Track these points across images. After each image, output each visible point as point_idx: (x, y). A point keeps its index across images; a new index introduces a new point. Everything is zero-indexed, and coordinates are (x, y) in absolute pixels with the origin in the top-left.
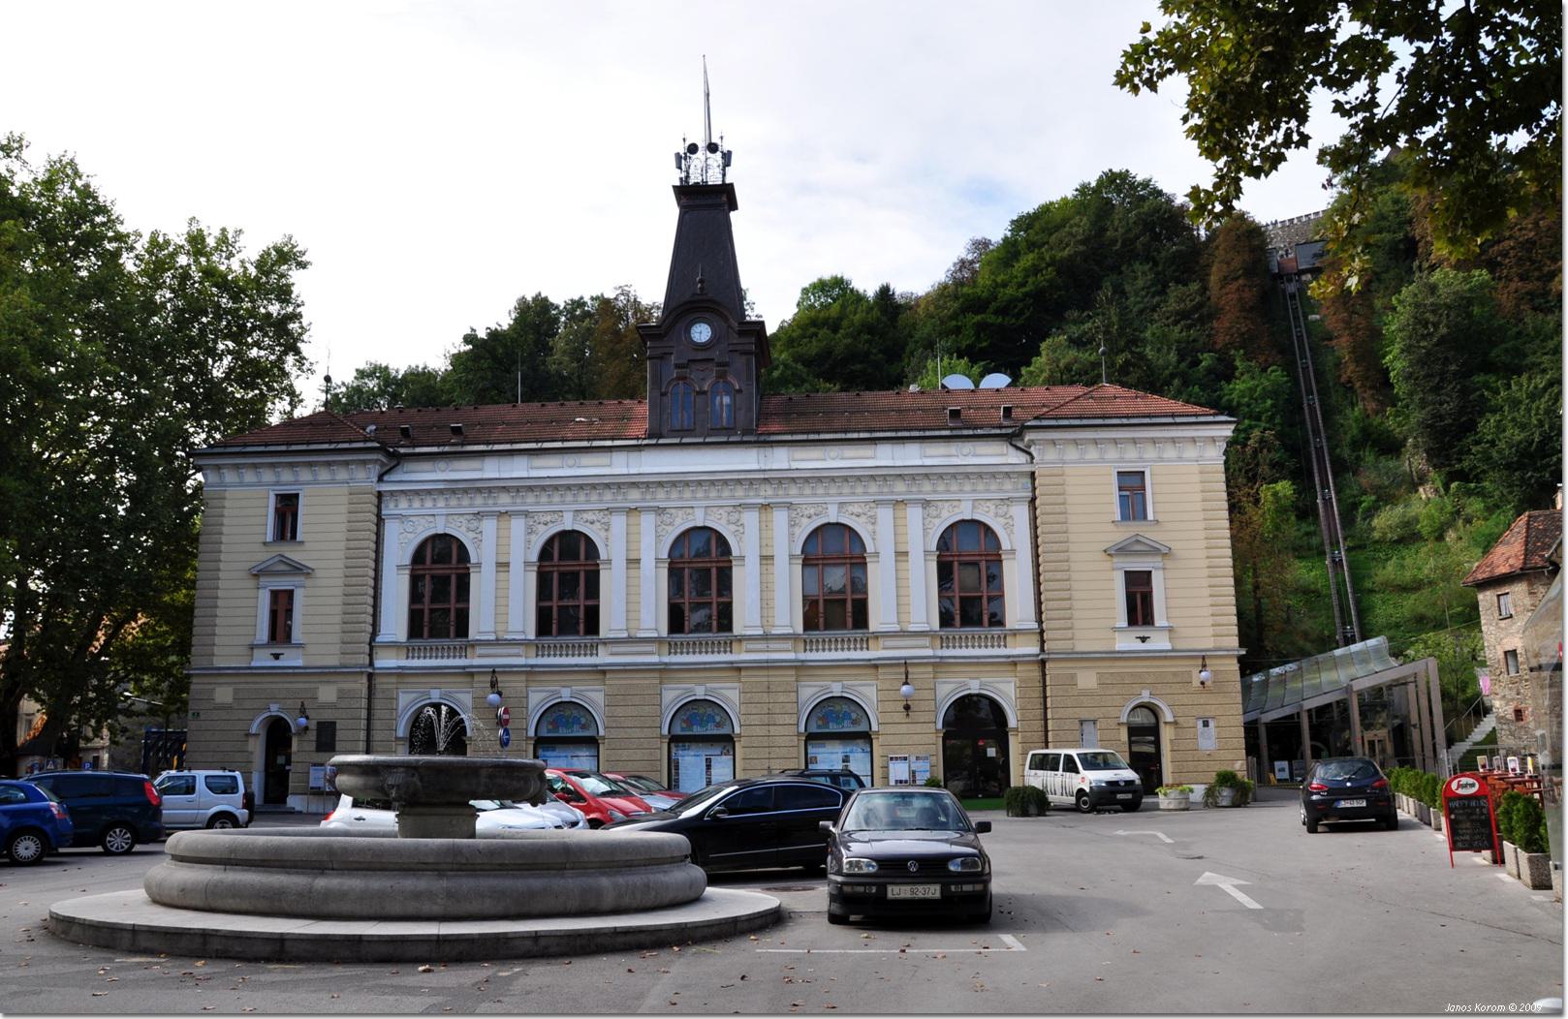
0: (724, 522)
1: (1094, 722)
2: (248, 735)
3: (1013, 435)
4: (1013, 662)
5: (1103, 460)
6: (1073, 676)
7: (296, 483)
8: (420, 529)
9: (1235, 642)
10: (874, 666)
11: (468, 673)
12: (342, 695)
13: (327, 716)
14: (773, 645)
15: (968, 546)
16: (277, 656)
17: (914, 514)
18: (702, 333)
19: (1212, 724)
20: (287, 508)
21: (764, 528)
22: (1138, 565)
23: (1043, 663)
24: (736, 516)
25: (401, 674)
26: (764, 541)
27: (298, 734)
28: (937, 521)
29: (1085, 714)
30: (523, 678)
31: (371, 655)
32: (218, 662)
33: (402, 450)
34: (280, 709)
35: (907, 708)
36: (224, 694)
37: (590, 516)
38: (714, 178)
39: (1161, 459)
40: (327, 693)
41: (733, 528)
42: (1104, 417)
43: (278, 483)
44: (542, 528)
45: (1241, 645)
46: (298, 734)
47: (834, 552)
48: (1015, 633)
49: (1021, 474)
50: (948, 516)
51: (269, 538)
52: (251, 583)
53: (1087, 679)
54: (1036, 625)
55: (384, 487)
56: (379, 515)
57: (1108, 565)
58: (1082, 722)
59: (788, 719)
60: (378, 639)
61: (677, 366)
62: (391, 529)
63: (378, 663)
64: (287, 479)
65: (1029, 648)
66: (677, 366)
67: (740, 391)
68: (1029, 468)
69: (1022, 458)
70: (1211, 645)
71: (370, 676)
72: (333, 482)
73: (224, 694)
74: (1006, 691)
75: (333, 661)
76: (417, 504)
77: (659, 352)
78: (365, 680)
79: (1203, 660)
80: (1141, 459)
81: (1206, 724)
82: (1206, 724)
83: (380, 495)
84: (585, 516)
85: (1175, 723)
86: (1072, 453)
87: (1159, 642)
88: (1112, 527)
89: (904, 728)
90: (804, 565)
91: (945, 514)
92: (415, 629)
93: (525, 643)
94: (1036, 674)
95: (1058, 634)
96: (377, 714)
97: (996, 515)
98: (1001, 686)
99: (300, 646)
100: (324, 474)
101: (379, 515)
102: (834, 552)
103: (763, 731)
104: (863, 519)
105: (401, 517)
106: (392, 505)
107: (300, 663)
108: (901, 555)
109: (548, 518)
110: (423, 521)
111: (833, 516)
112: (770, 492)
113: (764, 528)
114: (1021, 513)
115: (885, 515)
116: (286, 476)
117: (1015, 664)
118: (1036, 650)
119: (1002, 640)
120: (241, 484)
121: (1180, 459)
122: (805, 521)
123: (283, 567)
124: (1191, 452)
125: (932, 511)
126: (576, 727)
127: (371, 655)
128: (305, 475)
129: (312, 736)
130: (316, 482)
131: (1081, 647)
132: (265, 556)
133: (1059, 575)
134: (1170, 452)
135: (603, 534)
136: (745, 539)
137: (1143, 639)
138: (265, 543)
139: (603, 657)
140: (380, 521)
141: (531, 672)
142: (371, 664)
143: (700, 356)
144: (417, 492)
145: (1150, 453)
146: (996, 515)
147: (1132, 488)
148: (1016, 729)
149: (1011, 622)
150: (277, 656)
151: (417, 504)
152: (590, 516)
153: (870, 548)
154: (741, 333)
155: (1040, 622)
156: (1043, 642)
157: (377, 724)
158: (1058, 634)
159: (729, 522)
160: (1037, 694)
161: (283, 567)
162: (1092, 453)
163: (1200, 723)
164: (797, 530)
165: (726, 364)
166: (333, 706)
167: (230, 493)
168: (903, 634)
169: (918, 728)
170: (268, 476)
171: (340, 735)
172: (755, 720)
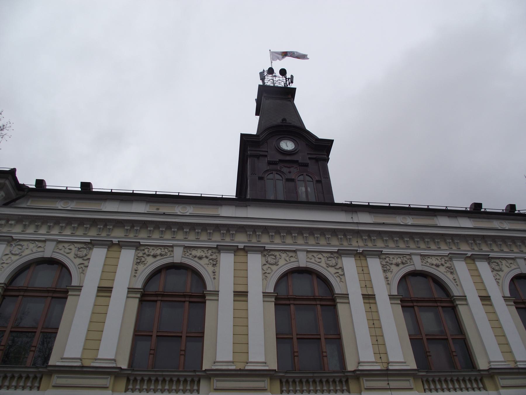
0: (71, 256)
15: (301, 287)
17: (255, 261)
24: (84, 252)
28: (274, 268)
41: (78, 261)
50: (284, 264)
90: (141, 301)
91: (282, 262)
97: (328, 266)
104: (205, 261)
108: (241, 295)
111: (178, 256)
115: (227, 260)
122: (150, 260)
153: (210, 287)
164: (141, 267)
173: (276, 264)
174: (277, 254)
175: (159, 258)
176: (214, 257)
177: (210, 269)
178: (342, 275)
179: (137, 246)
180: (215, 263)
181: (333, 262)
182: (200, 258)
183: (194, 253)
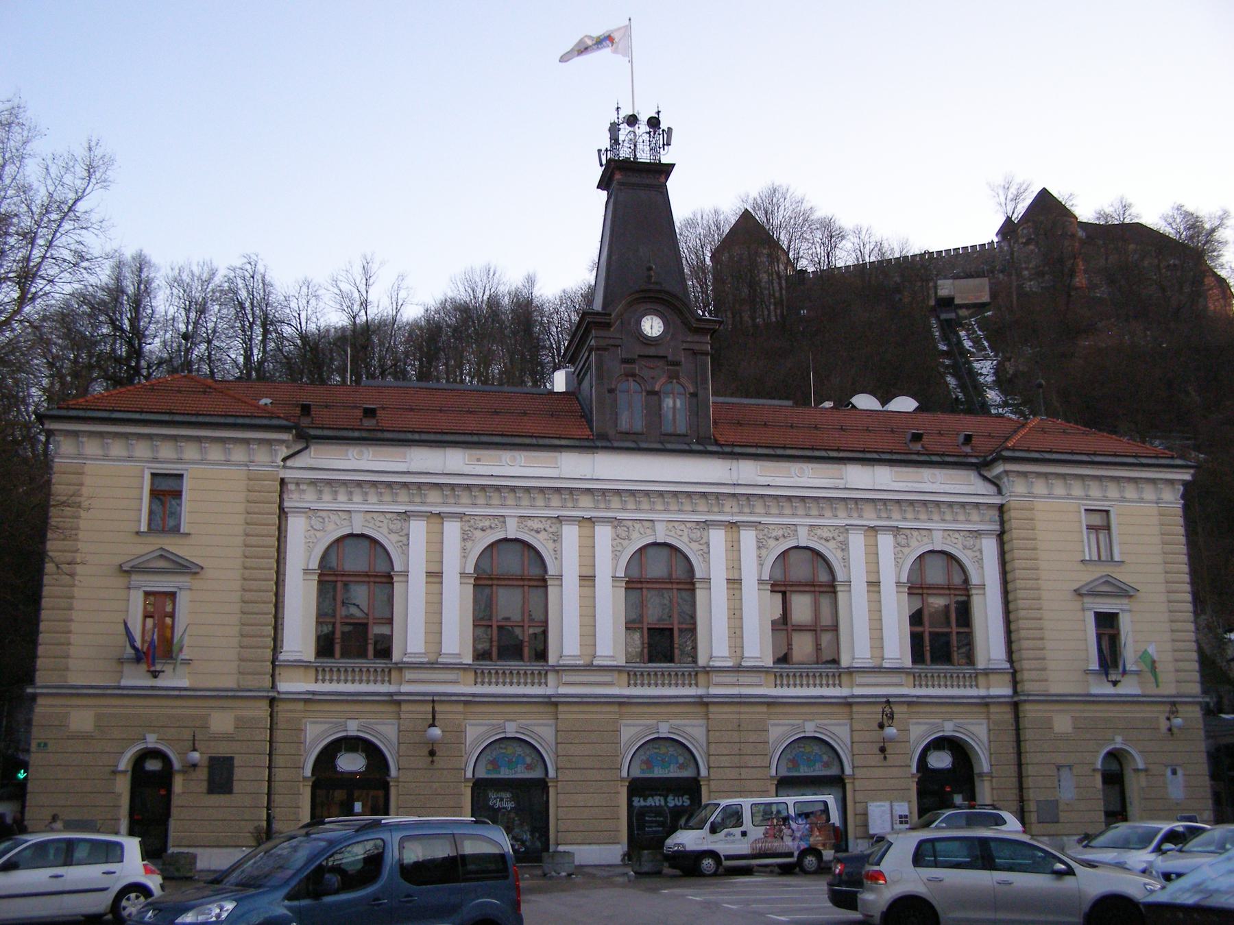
0: (685, 539)
1: (1070, 767)
2: (115, 772)
3: (981, 466)
4: (985, 703)
5: (1069, 497)
6: (1050, 719)
7: (180, 461)
8: (331, 527)
9: (1196, 688)
10: (847, 703)
11: (394, 701)
12: (240, 724)
13: (222, 749)
14: (744, 679)
16: (155, 675)
17: (886, 542)
18: (652, 326)
19: (1180, 772)
20: (166, 491)
21: (734, 547)
22: (1107, 606)
23: (1016, 705)
25: (310, 699)
26: (735, 563)
27: (184, 772)
28: (906, 550)
29: (1060, 759)
30: (460, 708)
31: (273, 676)
32: (75, 679)
33: (312, 432)
34: (160, 740)
35: (883, 750)
36: (82, 719)
37: (535, 524)
38: (644, 156)
39: (1123, 499)
40: (222, 721)
41: (695, 546)
42: (1072, 453)
43: (155, 460)
44: (478, 534)
45: (1205, 692)
46: (184, 772)
47: (805, 580)
48: (987, 672)
49: (990, 506)
51: (144, 528)
52: (121, 581)
53: (1062, 723)
54: (1008, 665)
55: (287, 474)
56: (281, 509)
57: (1078, 605)
58: (1059, 768)
59: (759, 761)
60: (282, 657)
61: (625, 361)
62: (297, 527)
63: (283, 686)
64: (167, 456)
65: (1001, 689)
66: (625, 361)
67: (694, 395)
68: (997, 500)
69: (991, 489)
70: (1173, 692)
71: (272, 701)
72: (227, 462)
73: (82, 719)
74: (977, 733)
75: (229, 682)
76: (327, 496)
77: (602, 343)
78: (265, 705)
79: (1173, 705)
80: (1105, 498)
81: (1174, 772)
82: (1174, 772)
83: (283, 482)
84: (530, 523)
85: (1146, 770)
86: (1040, 487)
87: (1129, 687)
88: (1082, 567)
89: (879, 772)
92: (325, 647)
93: (464, 668)
94: (1009, 717)
95: (1034, 675)
96: (280, 747)
97: (965, 547)
98: (971, 728)
99: (187, 662)
100: (215, 453)
101: (281, 509)
102: (805, 580)
103: (732, 774)
104: (832, 544)
105: (309, 512)
106: (295, 496)
107: (185, 683)
109: (487, 523)
110: (333, 517)
112: (735, 510)
113: (734, 547)
114: (990, 546)
116: (166, 451)
117: (987, 705)
118: (1008, 691)
119: (975, 678)
120: (106, 457)
121: (1142, 500)
122: (772, 543)
123: (162, 564)
124: (1149, 493)
125: (901, 539)
126: (520, 768)
127: (273, 676)
128: (191, 452)
129: (202, 774)
130: (203, 461)
131: (1054, 689)
132: (141, 550)
133: (1033, 614)
134: (1130, 492)
135: (551, 545)
136: (714, 558)
137: (1115, 683)
138: (137, 533)
139: (551, 688)
140: (282, 513)
141: (469, 701)
142: (274, 686)
143: (652, 351)
144: (329, 482)
145: (1113, 491)
146: (965, 547)
147: (1101, 524)
148: (990, 775)
149: (981, 663)
150: (155, 675)
151: (327, 496)
152: (535, 524)
153: (840, 576)
154: (697, 331)
155: (1010, 659)
156: (1015, 683)
157: (279, 760)
158: (1034, 675)
159: (691, 540)
160: (1010, 737)
161: (162, 564)
162: (1059, 489)
163: (1169, 772)
165: (678, 364)
166: (229, 738)
167: (90, 467)
168: (878, 670)
169: (895, 772)
170: (142, 450)
171: (238, 773)
172: (725, 761)
173: (908, 546)
174: (908, 532)
175: (781, 540)
176: (841, 539)
177: (839, 554)
178: (980, 561)
179: (756, 525)
180: (844, 546)
181: (970, 542)
182: (827, 540)
183: (819, 532)
